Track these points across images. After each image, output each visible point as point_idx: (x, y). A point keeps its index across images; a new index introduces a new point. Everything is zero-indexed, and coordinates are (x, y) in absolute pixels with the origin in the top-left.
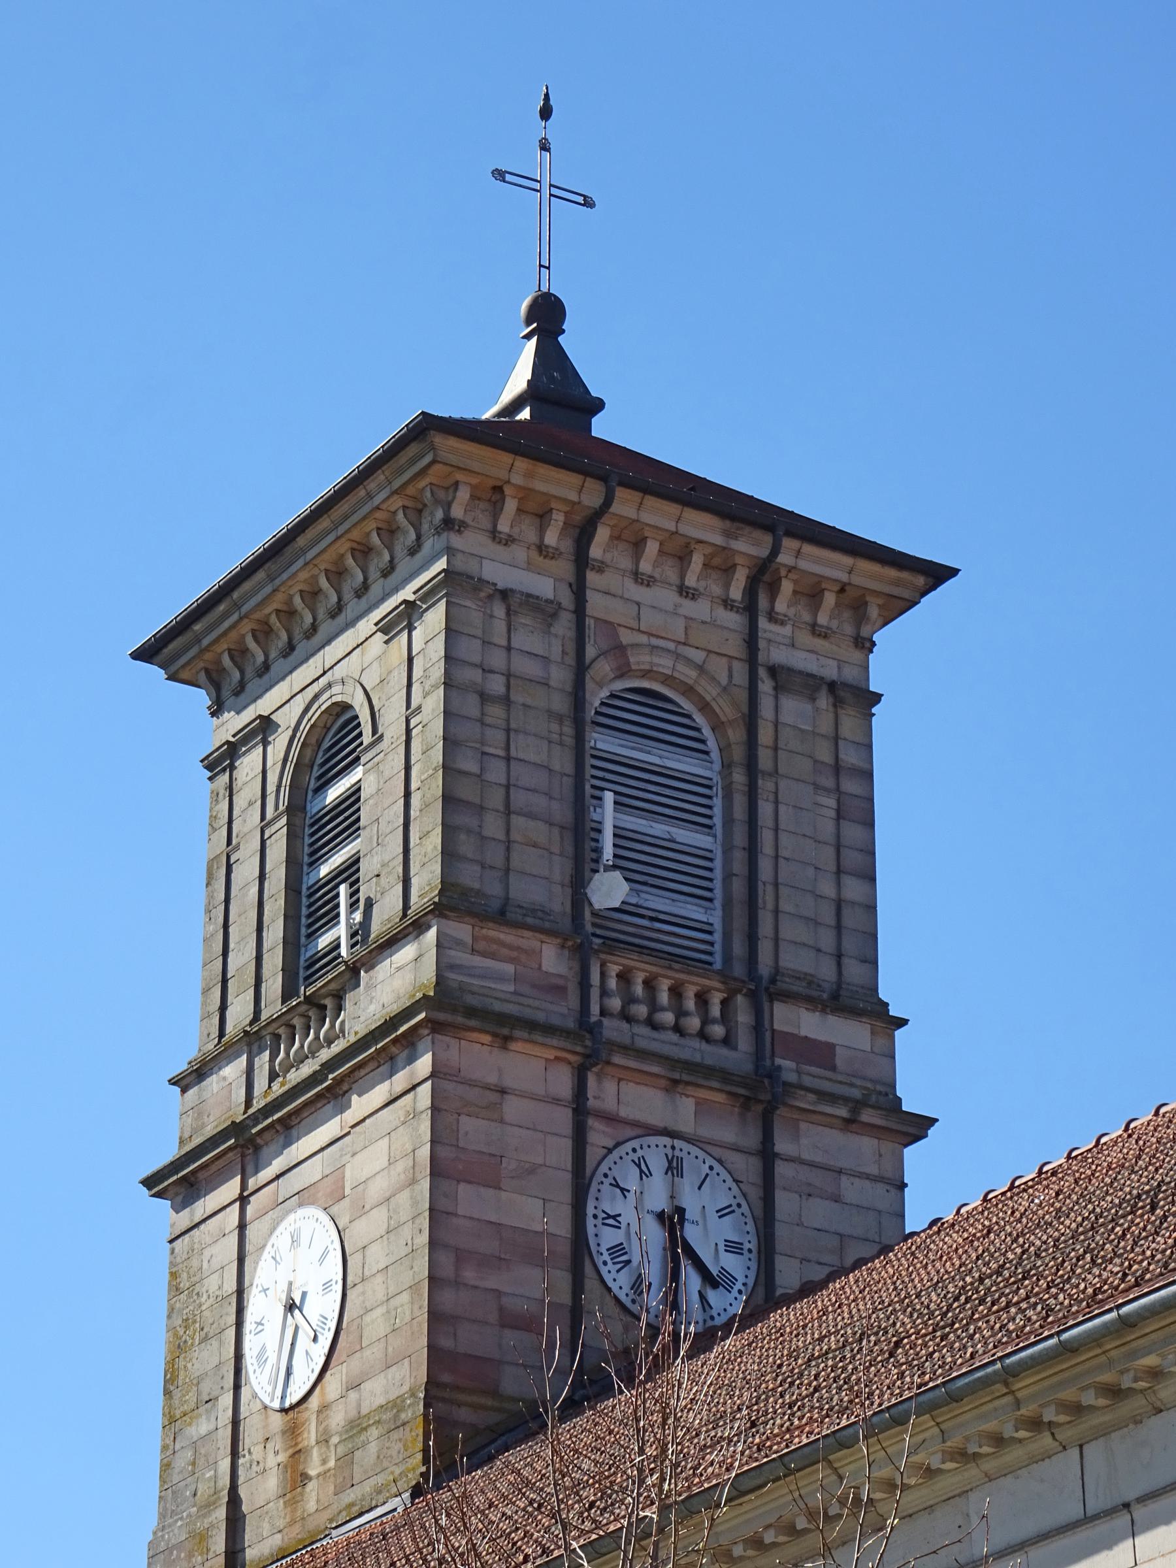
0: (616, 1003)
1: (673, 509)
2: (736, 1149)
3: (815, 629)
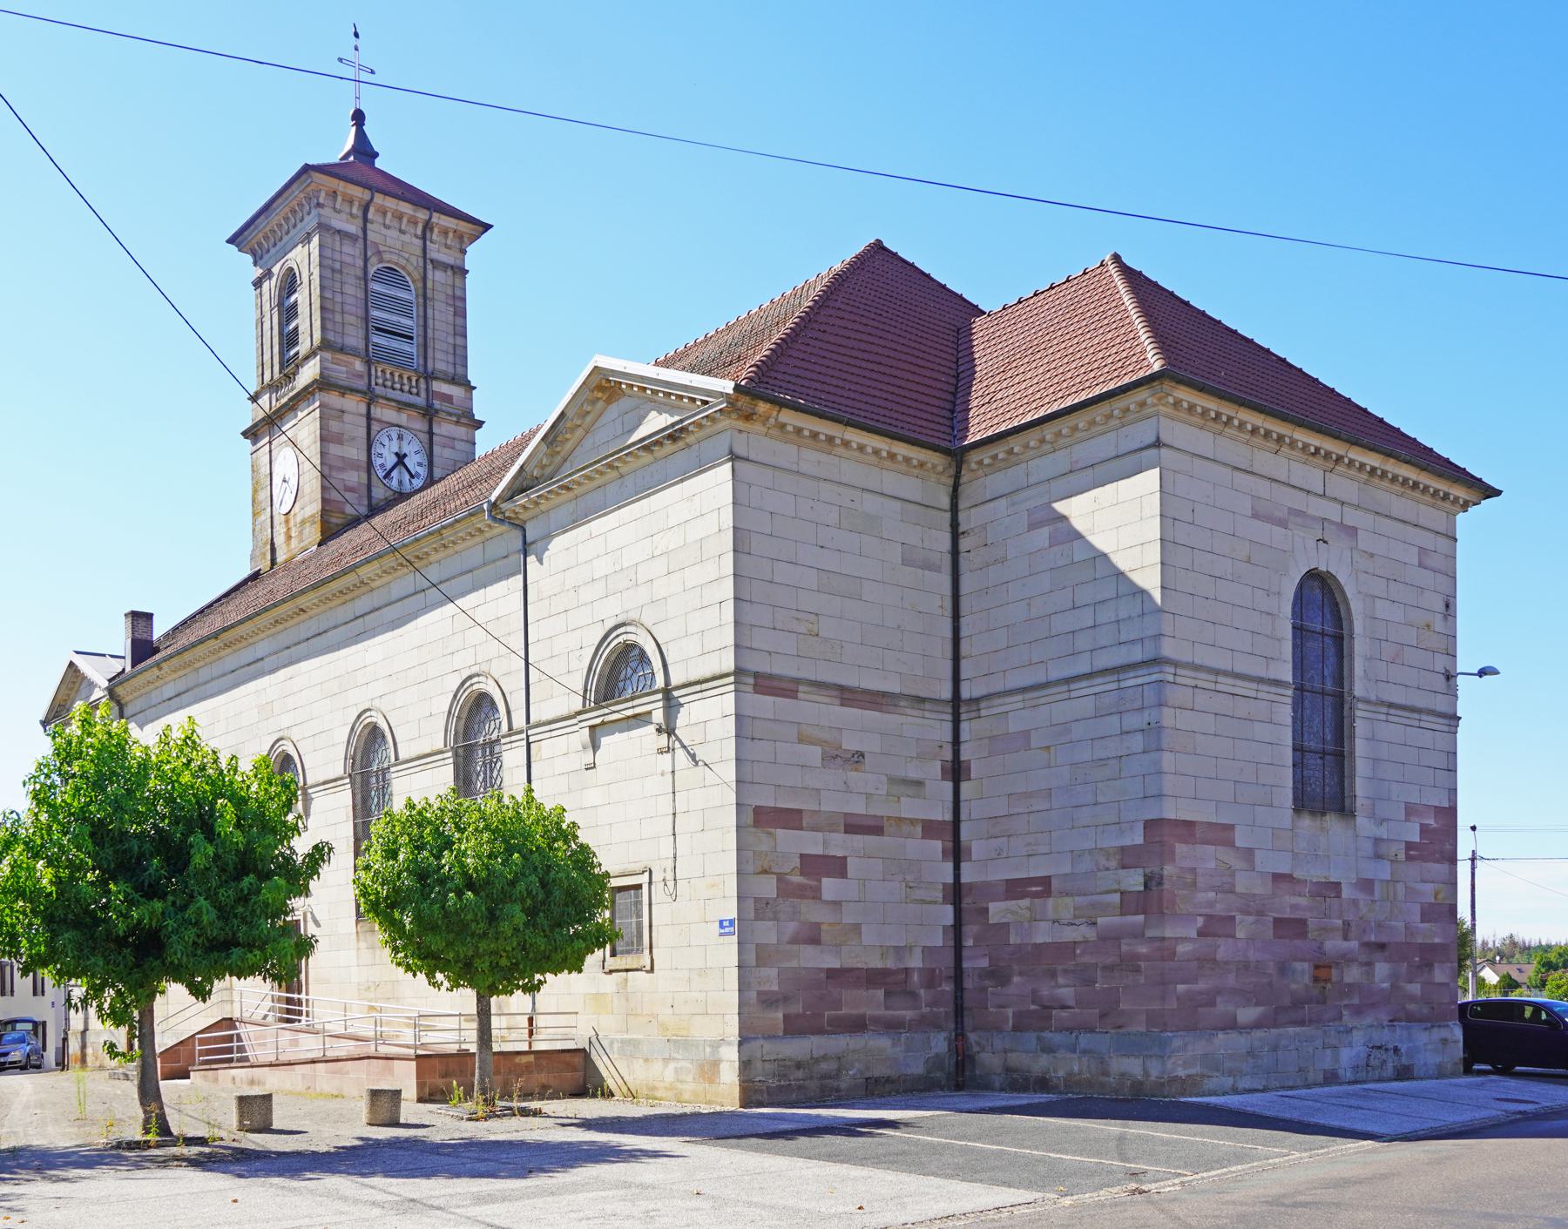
0: (380, 381)
1: (396, 201)
3: (447, 246)
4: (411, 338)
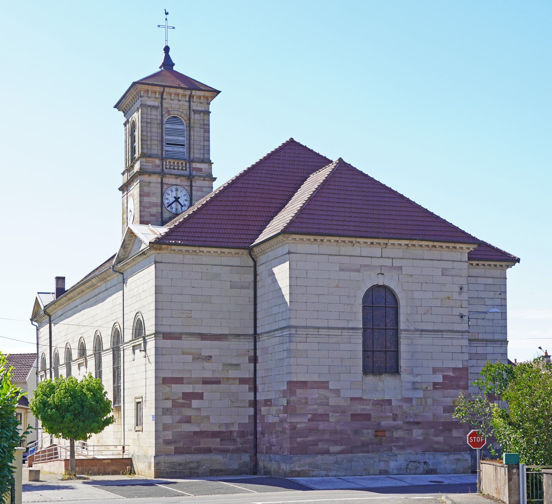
0: (168, 167)
2: (187, 186)
3: (200, 103)
4: (184, 145)
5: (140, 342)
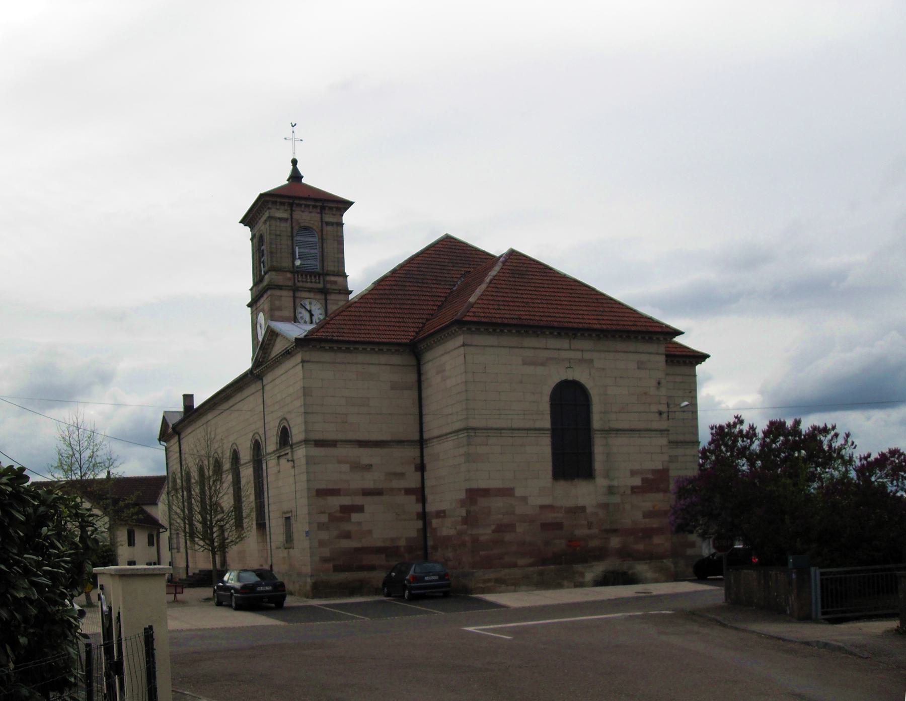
5: (286, 452)
